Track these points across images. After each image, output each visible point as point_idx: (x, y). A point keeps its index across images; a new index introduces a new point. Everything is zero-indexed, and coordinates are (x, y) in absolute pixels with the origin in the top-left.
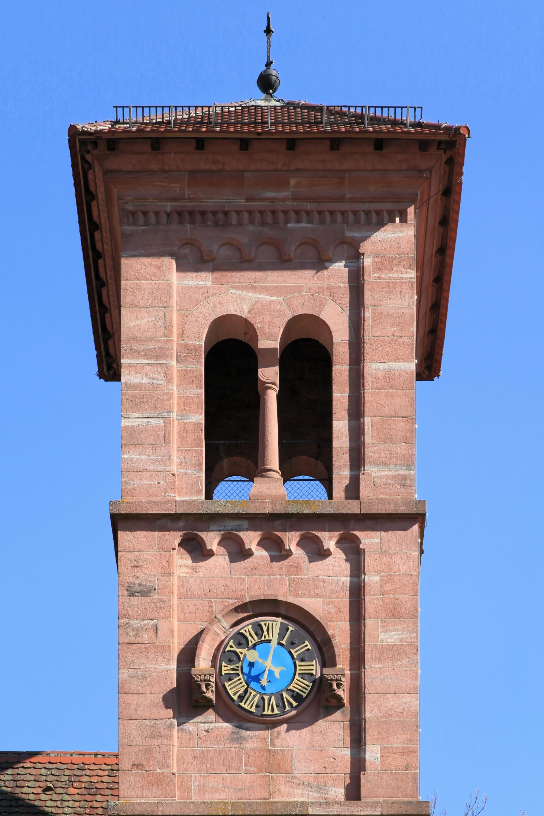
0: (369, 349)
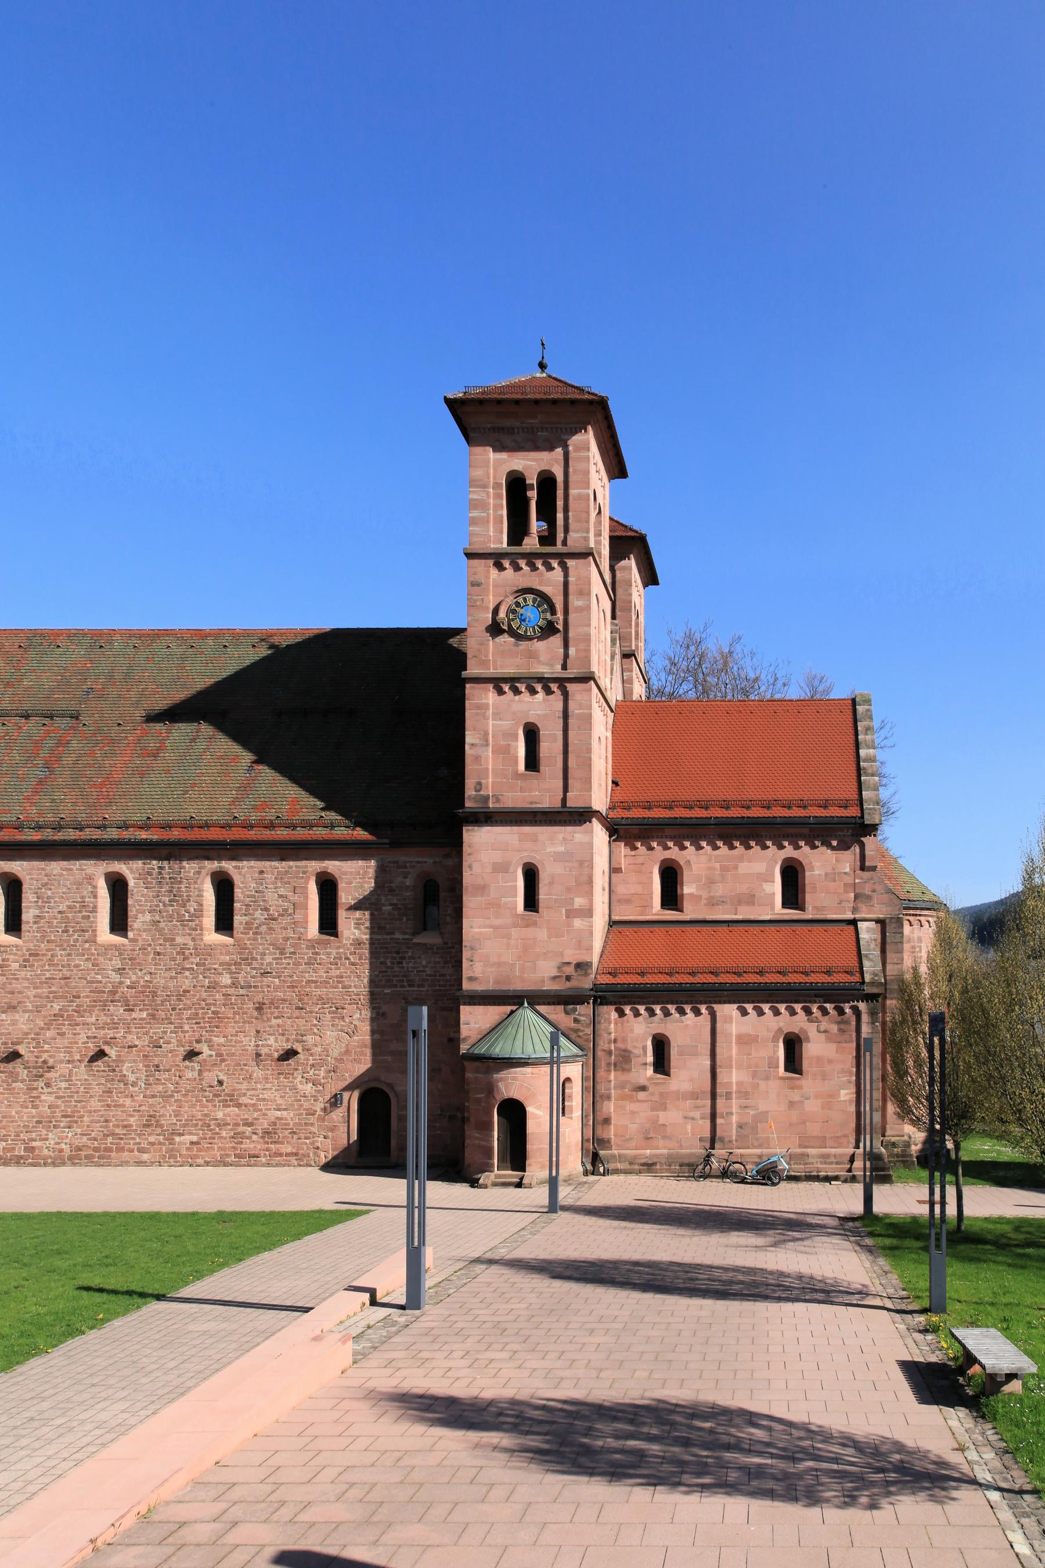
0: (571, 484)
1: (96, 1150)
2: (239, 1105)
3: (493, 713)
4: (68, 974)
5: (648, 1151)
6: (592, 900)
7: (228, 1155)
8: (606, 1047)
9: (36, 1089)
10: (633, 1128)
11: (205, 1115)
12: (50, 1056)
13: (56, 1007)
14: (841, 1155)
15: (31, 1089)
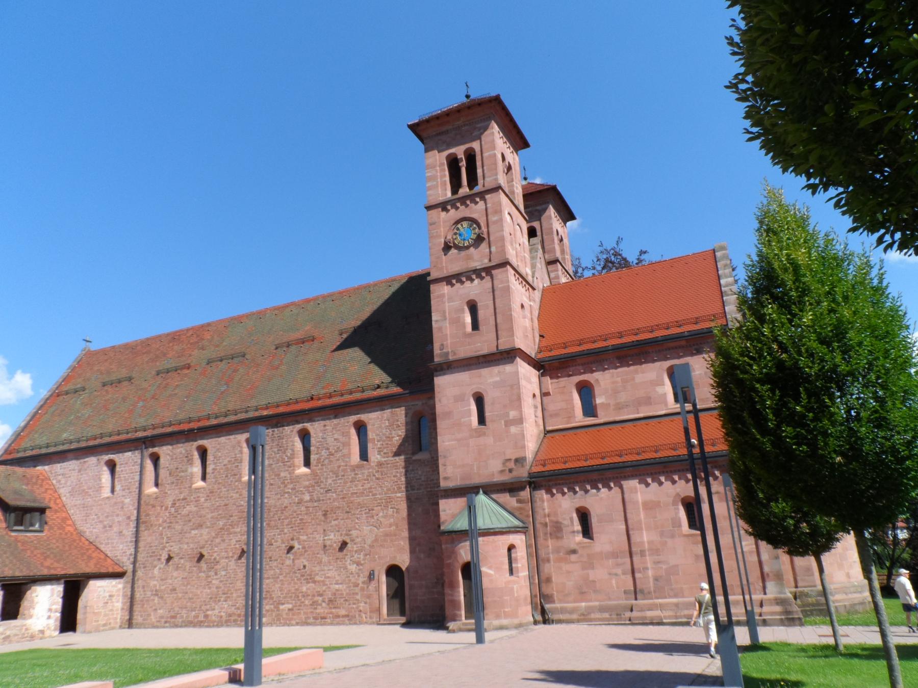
2: (314, 582)
3: (448, 299)
4: (227, 502)
5: (583, 604)
6: (521, 412)
7: (309, 618)
8: (542, 520)
10: (570, 584)
13: (221, 523)
15: (208, 577)
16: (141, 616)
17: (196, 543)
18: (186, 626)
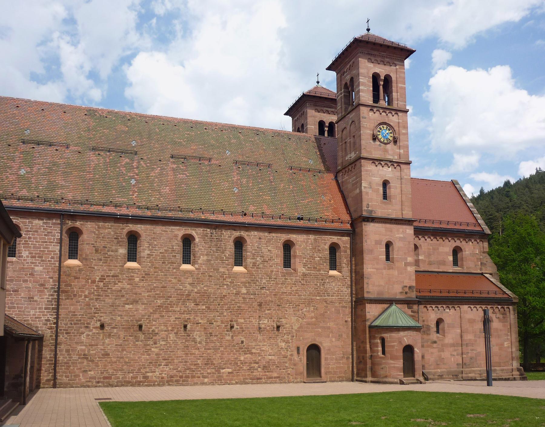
1: (181, 377)
2: (252, 353)
7: (247, 379)
9: (149, 345)
11: (236, 358)
12: (156, 328)
13: (159, 302)
14: (508, 369)
16: (66, 377)
17: (131, 316)
18: (122, 385)
